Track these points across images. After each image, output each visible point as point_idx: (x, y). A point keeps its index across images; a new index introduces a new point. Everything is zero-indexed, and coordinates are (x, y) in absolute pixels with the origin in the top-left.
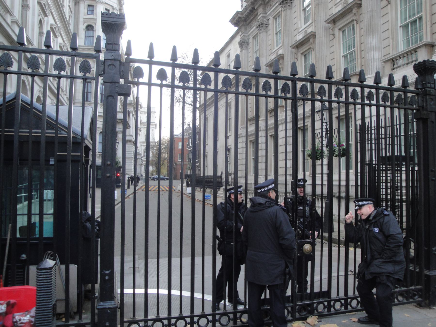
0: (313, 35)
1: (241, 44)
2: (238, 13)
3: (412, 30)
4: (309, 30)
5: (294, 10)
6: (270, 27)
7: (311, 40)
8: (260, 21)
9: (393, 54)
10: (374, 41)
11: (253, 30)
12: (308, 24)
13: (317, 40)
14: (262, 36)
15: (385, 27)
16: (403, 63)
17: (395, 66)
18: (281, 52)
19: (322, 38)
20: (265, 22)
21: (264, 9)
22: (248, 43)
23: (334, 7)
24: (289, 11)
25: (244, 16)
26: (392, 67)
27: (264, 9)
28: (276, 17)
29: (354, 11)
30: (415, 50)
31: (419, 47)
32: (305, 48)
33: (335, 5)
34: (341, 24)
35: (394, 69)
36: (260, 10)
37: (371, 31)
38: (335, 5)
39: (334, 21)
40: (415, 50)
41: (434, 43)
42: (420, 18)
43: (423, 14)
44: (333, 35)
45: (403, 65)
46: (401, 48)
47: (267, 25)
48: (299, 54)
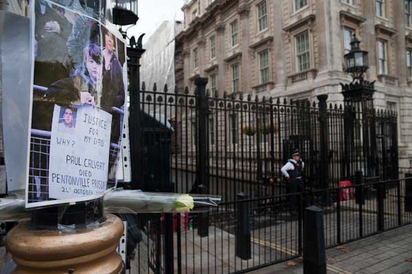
0: (240, 55)
2: (182, 32)
4: (237, 51)
5: (226, 35)
6: (207, 44)
7: (239, 58)
8: (200, 40)
9: (292, 73)
10: (281, 64)
12: (235, 46)
13: (243, 58)
14: (201, 51)
18: (215, 63)
19: (246, 56)
21: (203, 32)
22: (189, 54)
24: (222, 37)
25: (187, 34)
27: (203, 32)
29: (268, 43)
31: (308, 71)
32: (234, 62)
34: (260, 49)
35: (293, 82)
36: (200, 32)
37: (279, 57)
39: (255, 47)
40: (306, 73)
42: (308, 53)
43: (310, 50)
44: (254, 56)
46: (297, 71)
47: (205, 43)
48: (230, 66)
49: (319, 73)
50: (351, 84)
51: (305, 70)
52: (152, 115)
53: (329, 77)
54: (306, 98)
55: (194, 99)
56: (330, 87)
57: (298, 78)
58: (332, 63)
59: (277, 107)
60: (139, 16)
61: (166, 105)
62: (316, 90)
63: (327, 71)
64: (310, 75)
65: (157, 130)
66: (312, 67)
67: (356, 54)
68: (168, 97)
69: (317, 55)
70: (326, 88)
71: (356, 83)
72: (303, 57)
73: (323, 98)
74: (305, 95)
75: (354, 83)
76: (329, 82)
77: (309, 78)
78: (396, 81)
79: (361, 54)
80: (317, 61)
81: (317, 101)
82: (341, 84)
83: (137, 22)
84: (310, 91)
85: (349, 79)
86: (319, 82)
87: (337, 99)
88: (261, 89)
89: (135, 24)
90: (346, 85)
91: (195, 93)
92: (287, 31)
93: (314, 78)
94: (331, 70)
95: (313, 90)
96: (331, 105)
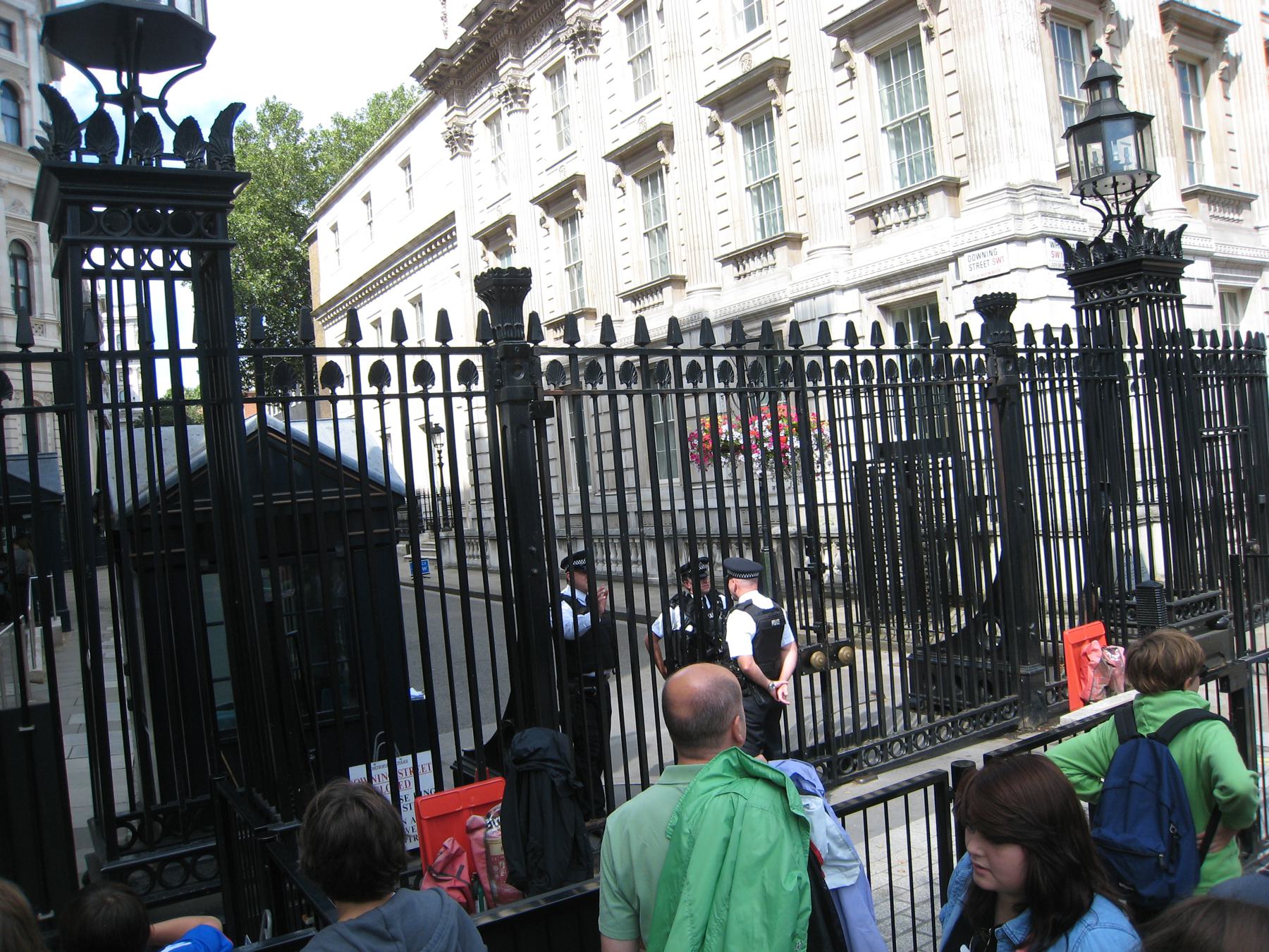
1: (451, 138)
2: (437, 54)
3: (908, 143)
5: (604, 60)
11: (485, 101)
15: (850, 129)
16: (898, 220)
17: (880, 225)
20: (522, 84)
23: (717, 67)
26: (874, 228)
28: (555, 72)
30: (922, 194)
33: (719, 63)
35: (877, 232)
38: (719, 63)
39: (722, 102)
45: (898, 224)
46: (890, 187)
50: (1099, 241)
51: (919, 185)
52: (301, 428)
54: (929, 290)
55: (477, 360)
57: (892, 217)
59: (819, 360)
60: (212, 30)
61: (358, 398)
65: (330, 494)
68: (366, 362)
71: (1118, 236)
72: (911, 131)
73: (996, 308)
74: (921, 281)
75: (1108, 238)
76: (1012, 229)
77: (932, 215)
79: (1127, 125)
81: (976, 323)
82: (1061, 241)
83: (211, 57)
84: (941, 265)
85: (1086, 222)
87: (1047, 307)
88: (753, 264)
89: (203, 63)
90: (1080, 245)
91: (481, 336)
92: (840, 35)
93: (956, 215)
96: (1029, 330)
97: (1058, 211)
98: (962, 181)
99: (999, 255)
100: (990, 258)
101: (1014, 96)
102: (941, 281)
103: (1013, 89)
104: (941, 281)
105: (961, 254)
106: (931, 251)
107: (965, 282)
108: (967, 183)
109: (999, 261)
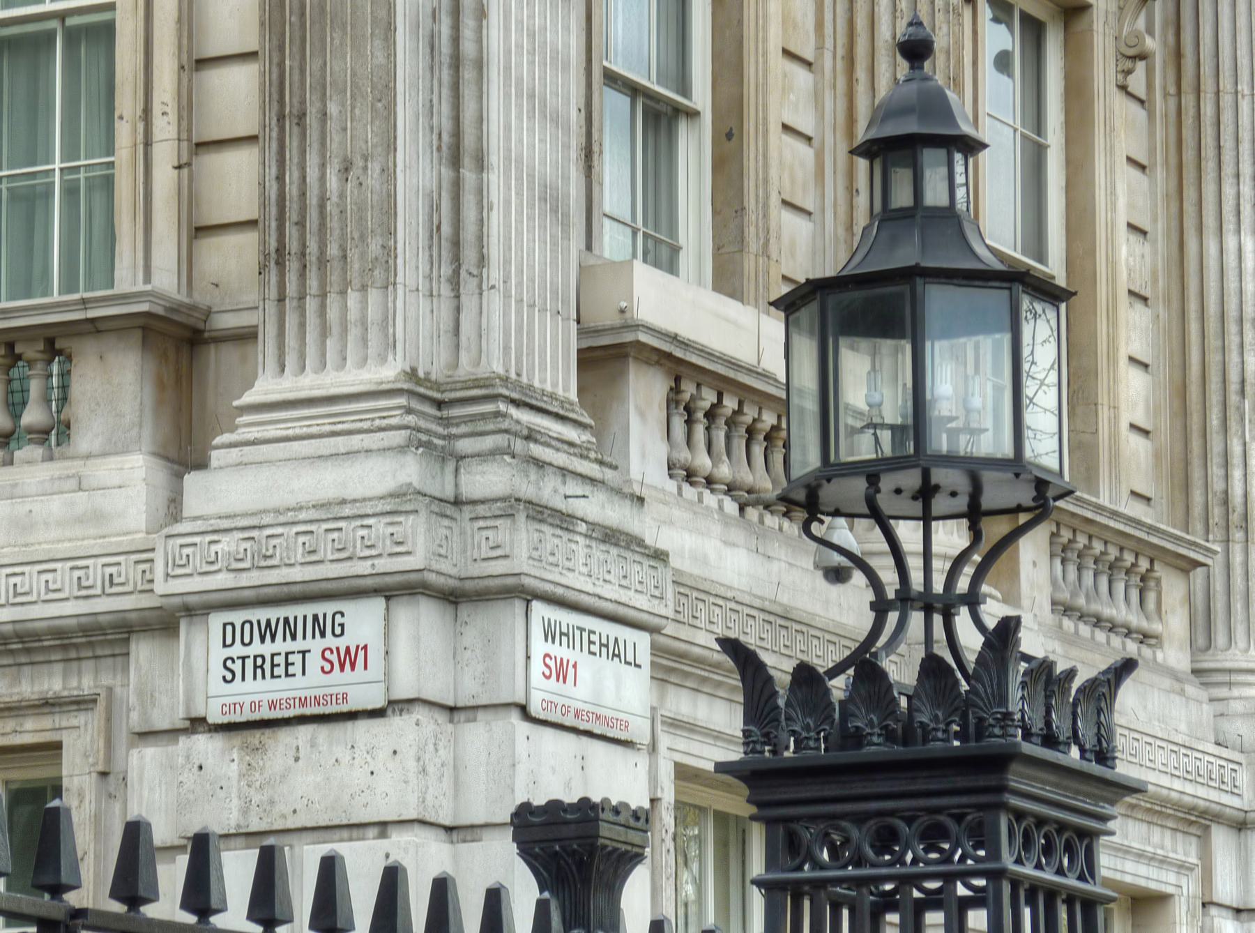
31: (95, 328)
40: (55, 343)
41: (208, 313)
49: (268, 386)
50: (864, 664)
53: (410, 471)
54: (30, 731)
56: (420, 623)
58: (459, 255)
62: (206, 646)
63: (388, 372)
64: (113, 391)
66: (148, 269)
67: (938, 299)
69: (235, 96)
70: (363, 622)
75: (902, 669)
77: (85, 438)
78: (1172, 588)
80: (236, 182)
84: (107, 638)
86: (249, 525)
90: (805, 676)
94: (434, 364)
95: (166, 622)
97: (580, 507)
98: (227, 322)
99: (350, 640)
100: (316, 645)
101: (468, 48)
102: (82, 703)
103: (468, 24)
104: (82, 703)
105: (195, 610)
106: (63, 576)
107: (197, 724)
108: (248, 336)
109: (348, 659)
